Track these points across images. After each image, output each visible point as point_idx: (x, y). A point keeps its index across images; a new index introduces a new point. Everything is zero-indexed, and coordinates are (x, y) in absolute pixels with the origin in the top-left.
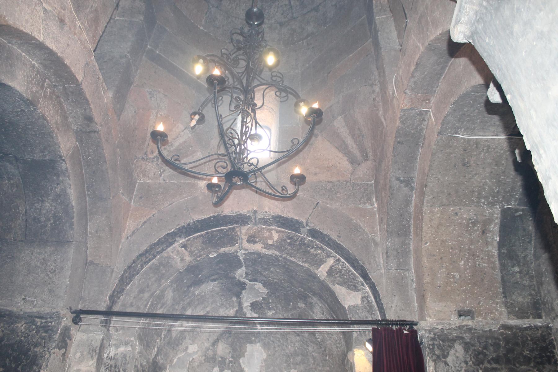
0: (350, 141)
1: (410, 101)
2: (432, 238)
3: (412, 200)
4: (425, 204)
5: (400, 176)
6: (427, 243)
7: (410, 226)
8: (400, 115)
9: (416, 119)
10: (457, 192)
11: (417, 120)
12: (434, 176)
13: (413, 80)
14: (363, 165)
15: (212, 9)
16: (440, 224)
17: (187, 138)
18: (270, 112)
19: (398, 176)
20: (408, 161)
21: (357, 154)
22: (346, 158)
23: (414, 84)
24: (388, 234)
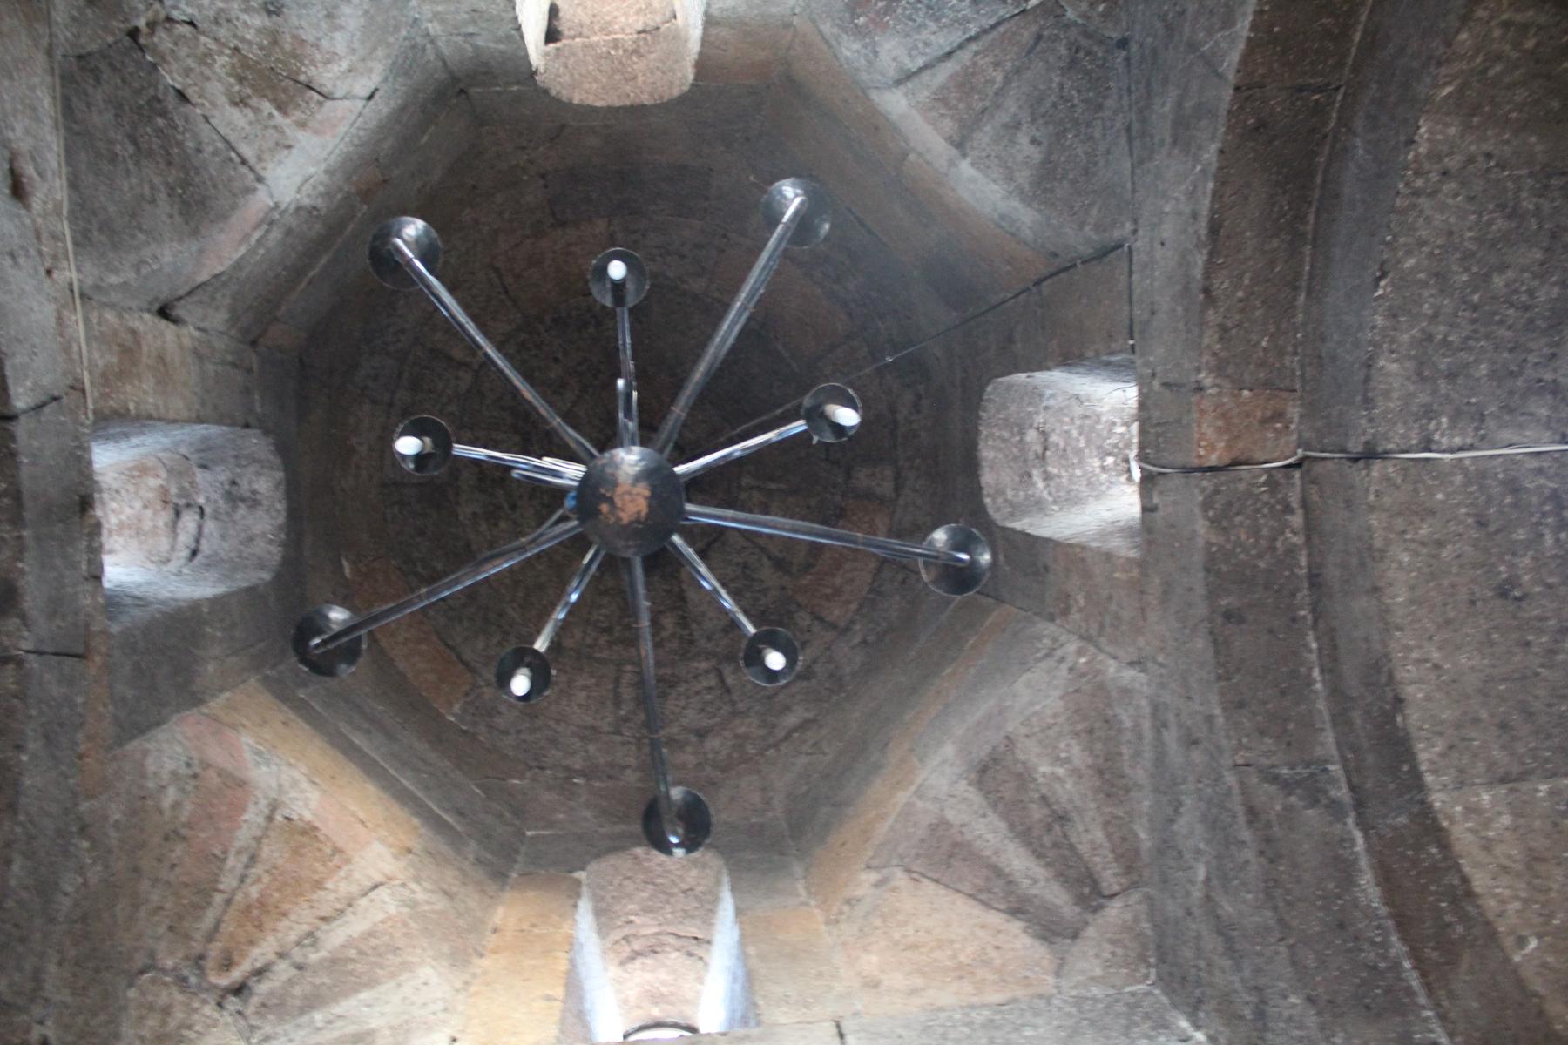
0: (1018, 861)
1: (1220, 423)
2: (1537, 920)
3: (1356, 861)
4: (1429, 778)
5: (1274, 760)
6: (1522, 942)
7: (1396, 966)
8: (1203, 490)
9: (1258, 511)
10: (1529, 715)
11: (1266, 511)
12: (1415, 655)
13: (1212, 316)
14: (1090, 932)
15: (485, 689)
16: (1534, 859)
17: (381, 916)
18: (690, 954)
19: (1265, 761)
20: (1283, 693)
21: (1058, 897)
22: (1016, 926)
23: (1221, 339)
24: (1320, 1013)
